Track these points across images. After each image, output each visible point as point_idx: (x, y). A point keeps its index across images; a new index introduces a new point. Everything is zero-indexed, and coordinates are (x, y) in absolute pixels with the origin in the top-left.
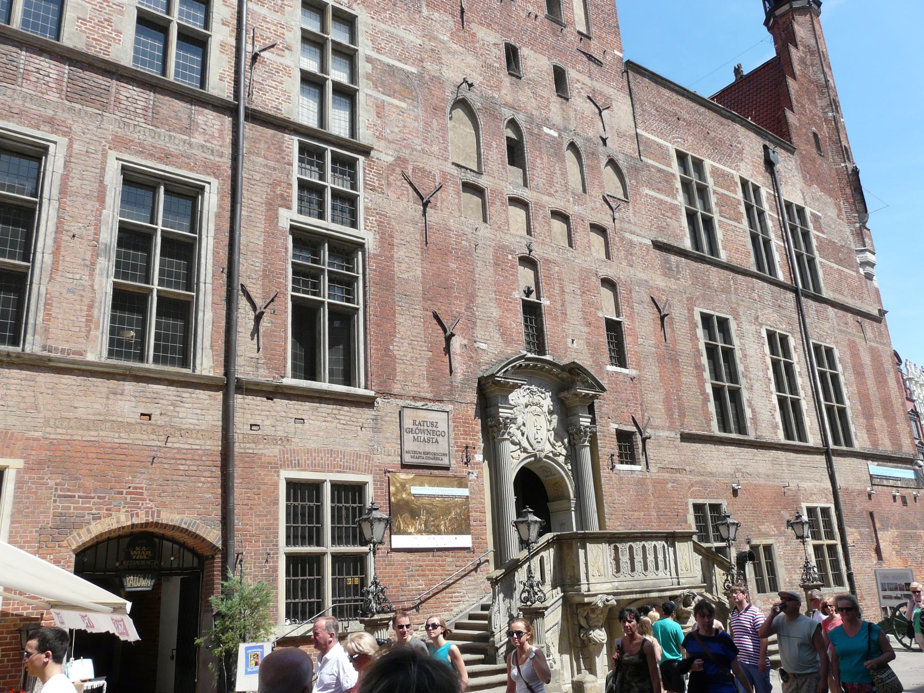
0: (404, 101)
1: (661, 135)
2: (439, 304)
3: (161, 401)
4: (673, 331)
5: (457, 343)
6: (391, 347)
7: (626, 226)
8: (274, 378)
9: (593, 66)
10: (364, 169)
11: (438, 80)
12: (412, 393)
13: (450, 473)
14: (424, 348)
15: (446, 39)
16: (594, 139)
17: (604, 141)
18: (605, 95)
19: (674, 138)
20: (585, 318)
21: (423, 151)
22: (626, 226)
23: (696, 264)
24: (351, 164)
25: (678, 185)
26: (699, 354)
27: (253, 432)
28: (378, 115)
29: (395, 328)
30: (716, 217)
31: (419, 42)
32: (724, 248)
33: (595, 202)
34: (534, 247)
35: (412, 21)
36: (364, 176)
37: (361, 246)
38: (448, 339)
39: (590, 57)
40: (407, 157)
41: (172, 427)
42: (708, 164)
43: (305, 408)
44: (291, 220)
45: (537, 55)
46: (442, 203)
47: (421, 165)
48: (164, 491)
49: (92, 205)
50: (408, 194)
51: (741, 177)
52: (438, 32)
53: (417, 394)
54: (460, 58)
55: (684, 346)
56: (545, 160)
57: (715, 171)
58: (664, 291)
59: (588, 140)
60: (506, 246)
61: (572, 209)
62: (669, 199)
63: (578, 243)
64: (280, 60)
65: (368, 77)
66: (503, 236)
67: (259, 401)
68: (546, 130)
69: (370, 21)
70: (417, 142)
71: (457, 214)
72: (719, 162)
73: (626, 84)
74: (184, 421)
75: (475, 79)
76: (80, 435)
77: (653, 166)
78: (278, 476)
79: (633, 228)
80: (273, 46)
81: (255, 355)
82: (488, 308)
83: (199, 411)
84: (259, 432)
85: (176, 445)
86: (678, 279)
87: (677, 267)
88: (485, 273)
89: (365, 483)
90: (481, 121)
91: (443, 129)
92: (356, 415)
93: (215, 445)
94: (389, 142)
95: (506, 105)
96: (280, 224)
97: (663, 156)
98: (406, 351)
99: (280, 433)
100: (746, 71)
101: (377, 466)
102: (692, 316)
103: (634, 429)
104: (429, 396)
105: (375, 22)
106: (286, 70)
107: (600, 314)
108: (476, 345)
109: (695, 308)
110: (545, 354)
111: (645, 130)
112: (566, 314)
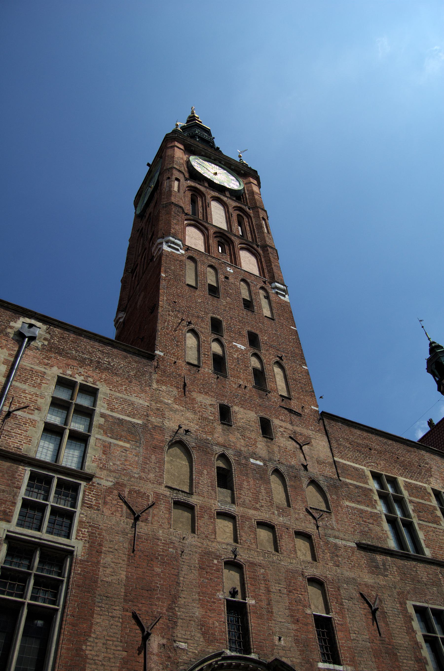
0: (128, 442)
1: (356, 461)
2: (140, 605)
4: (387, 625)
5: (155, 642)
6: (84, 647)
7: (330, 532)
9: (294, 417)
10: (85, 491)
11: (161, 429)
14: (119, 648)
15: (170, 402)
16: (297, 467)
17: (305, 467)
18: (305, 435)
19: (368, 463)
20: (292, 616)
21: (140, 478)
22: (330, 532)
23: (402, 562)
24: (75, 488)
25: (376, 497)
26: (418, 647)
28: (104, 453)
29: (91, 627)
30: (415, 521)
31: (147, 404)
32: (427, 546)
33: (299, 514)
34: (240, 551)
35: (143, 391)
36: (84, 497)
37: (71, 553)
38: (146, 637)
39: (291, 411)
40: (125, 482)
42: (401, 480)
44: (8, 531)
45: (245, 411)
46: (153, 517)
47: (137, 488)
50: (122, 511)
51: (432, 489)
52: (163, 397)
54: (181, 414)
55: (401, 640)
56: (252, 482)
57: (408, 486)
58: (372, 587)
59: (292, 467)
60: (212, 552)
61: (278, 520)
62: (369, 509)
63: (284, 548)
64: (31, 416)
65: (100, 427)
66: (210, 543)
68: (252, 460)
69: (108, 392)
70: (136, 471)
71: (166, 526)
72: (411, 478)
73: (322, 427)
75: (193, 427)
77: (351, 484)
79: (337, 533)
80: (25, 407)
82: (191, 607)
86: (387, 576)
87: (384, 565)
88: (189, 576)
90: (195, 456)
91: (161, 462)
94: (111, 471)
95: (218, 444)
97: (361, 476)
98: (99, 650)
100: (435, 422)
102: (406, 609)
105: (112, 393)
106: (33, 423)
107: (308, 612)
108: (175, 645)
109: (408, 602)
110: (250, 653)
111: (342, 458)
112: (272, 612)
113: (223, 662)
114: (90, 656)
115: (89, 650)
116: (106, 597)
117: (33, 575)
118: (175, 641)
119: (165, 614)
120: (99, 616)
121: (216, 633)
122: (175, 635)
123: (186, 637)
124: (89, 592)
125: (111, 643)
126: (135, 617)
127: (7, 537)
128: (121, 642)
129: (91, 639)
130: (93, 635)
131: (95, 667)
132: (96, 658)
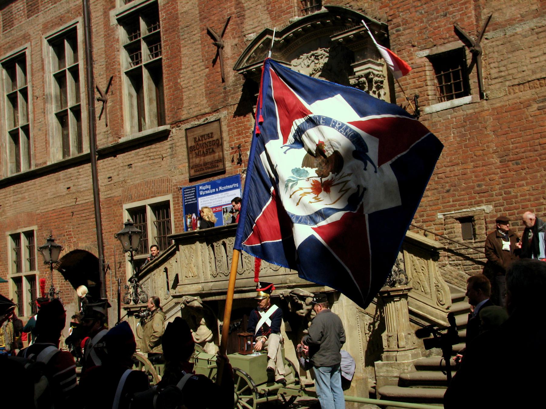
3: (73, 178)
8: (116, 140)
12: (195, 114)
13: (226, 176)
14: (204, 67)
27: (110, 183)
29: (181, 62)
41: (78, 192)
43: (133, 155)
48: (79, 231)
49: (41, 73)
53: (199, 113)
67: (109, 160)
74: (81, 186)
76: (51, 207)
81: (105, 129)
83: (86, 178)
84: (112, 182)
85: (81, 202)
89: (168, 202)
92: (160, 149)
93: (91, 198)
96: (111, 24)
98: (189, 78)
99: (122, 179)
101: (174, 186)
103: (460, 44)
104: (207, 110)
113: (288, 34)
114: (184, 86)
115: (183, 82)
116: (187, 27)
117: (142, 40)
118: (245, 36)
119: (233, 13)
120: (185, 48)
121: (283, 5)
122: (244, 30)
123: (254, 26)
124: (174, 31)
125: (195, 66)
126: (209, 33)
127: (119, 20)
128: (203, 61)
129: (182, 71)
130: (183, 67)
131: (188, 93)
132: (188, 85)
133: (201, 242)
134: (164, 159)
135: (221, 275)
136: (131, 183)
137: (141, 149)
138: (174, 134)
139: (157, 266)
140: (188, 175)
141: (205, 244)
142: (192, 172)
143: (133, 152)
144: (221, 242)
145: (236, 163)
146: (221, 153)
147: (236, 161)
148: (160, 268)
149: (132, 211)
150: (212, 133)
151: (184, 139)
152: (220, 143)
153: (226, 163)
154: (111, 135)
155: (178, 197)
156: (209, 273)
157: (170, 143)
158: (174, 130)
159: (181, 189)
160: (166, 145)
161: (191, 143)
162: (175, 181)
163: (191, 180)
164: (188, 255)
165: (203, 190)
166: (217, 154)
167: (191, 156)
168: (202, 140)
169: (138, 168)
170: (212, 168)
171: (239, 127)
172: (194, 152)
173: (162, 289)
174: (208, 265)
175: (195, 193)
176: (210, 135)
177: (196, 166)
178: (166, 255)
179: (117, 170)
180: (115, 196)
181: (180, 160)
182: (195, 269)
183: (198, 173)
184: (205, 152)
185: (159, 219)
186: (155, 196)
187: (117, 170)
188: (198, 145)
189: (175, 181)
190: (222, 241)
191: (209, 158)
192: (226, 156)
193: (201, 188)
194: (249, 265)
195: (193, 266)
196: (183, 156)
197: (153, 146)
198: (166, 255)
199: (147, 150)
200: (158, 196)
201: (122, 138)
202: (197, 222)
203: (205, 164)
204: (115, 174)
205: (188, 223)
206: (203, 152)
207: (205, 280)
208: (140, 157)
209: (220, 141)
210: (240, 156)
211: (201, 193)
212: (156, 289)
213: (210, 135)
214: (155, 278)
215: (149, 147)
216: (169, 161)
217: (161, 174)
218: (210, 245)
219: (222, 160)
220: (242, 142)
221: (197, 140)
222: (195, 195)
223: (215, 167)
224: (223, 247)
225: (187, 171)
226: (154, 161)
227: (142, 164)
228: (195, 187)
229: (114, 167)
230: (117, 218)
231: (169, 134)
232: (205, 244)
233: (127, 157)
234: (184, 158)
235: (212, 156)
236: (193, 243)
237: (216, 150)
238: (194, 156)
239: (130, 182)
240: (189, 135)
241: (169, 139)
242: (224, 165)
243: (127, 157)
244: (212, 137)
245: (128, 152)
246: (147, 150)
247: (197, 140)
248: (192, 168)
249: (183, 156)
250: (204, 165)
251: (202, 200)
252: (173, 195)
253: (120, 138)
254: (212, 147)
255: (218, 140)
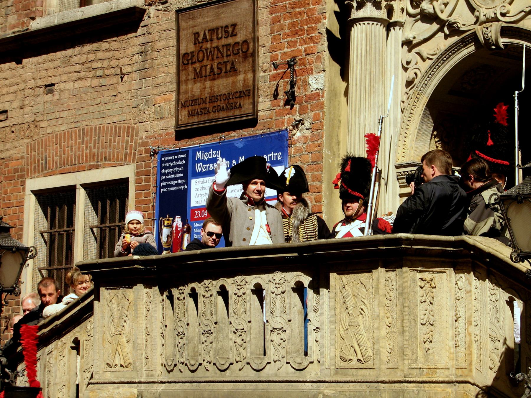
8: (23, 23)
13: (257, 131)
43: (57, 63)
78: (24, 189)
89: (126, 181)
92: (117, 54)
99: (28, 118)
101: (143, 144)
133: (149, 285)
134: (126, 78)
135: (210, 367)
136: (49, 130)
137: (77, 50)
138: (152, 20)
139: (58, 333)
140: (172, 122)
141: (156, 289)
142: (184, 113)
143: (60, 54)
144: (187, 289)
145: (282, 103)
146: (250, 75)
147: (282, 97)
148: (64, 339)
149: (44, 197)
150: (234, 25)
151: (173, 33)
152: (251, 51)
153: (261, 99)
154: (13, 9)
155: (148, 173)
156: (158, 360)
157: (142, 40)
158: (152, 10)
159: (155, 153)
160: (132, 42)
161: (188, 47)
162: (145, 134)
163: (182, 134)
164: (116, 314)
165: (204, 162)
166: (241, 77)
167: (183, 78)
168: (212, 40)
169: (66, 94)
170: (227, 109)
171: (296, 15)
172: (191, 68)
173: (65, 390)
174: (159, 341)
175: (186, 166)
176: (230, 29)
177: (194, 101)
178: (78, 308)
179: (20, 96)
180: (10, 158)
181: (159, 85)
182: (128, 348)
183: (196, 119)
184: (216, 70)
185: (103, 220)
186: (98, 167)
187: (20, 96)
188: (201, 50)
189: (145, 134)
190: (191, 285)
191: (222, 85)
192: (261, 84)
193: (198, 155)
194: (241, 349)
195: (125, 340)
196: (167, 74)
197: (104, 45)
198: (78, 308)
199: (89, 52)
200: (105, 166)
201: (38, 19)
202: (182, 237)
203: (214, 98)
204: (16, 104)
205: (164, 239)
206: (212, 68)
207: (148, 376)
208: (73, 69)
209: (251, 45)
210: (292, 84)
211: (198, 169)
212: (51, 388)
213: (230, 30)
214: (52, 361)
215: (95, 46)
216: (135, 85)
217: (115, 113)
218: (166, 293)
219: (250, 92)
220: (300, 51)
221: (200, 39)
222: (185, 172)
223: (235, 108)
224: (191, 301)
225: (173, 111)
226: (103, 81)
227: (77, 85)
228: (186, 152)
229: (15, 88)
230: (10, 211)
231: (141, 19)
232: (156, 289)
233: (46, 66)
234: (168, 79)
235: (230, 80)
236: (130, 284)
237: (240, 67)
238: (191, 76)
239: (47, 128)
240: (183, 24)
241: (140, 31)
242: (255, 104)
243: (46, 66)
244: (234, 35)
245: (47, 53)
246: (89, 52)
247: (200, 39)
248: (184, 106)
249: (167, 74)
250: (211, 101)
251: (200, 186)
252: (137, 167)
253: (33, 19)
254: (232, 58)
255: (245, 42)
